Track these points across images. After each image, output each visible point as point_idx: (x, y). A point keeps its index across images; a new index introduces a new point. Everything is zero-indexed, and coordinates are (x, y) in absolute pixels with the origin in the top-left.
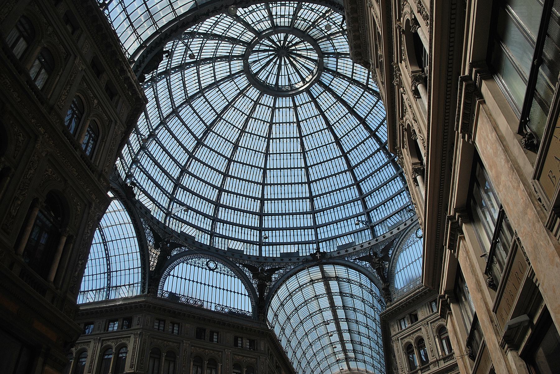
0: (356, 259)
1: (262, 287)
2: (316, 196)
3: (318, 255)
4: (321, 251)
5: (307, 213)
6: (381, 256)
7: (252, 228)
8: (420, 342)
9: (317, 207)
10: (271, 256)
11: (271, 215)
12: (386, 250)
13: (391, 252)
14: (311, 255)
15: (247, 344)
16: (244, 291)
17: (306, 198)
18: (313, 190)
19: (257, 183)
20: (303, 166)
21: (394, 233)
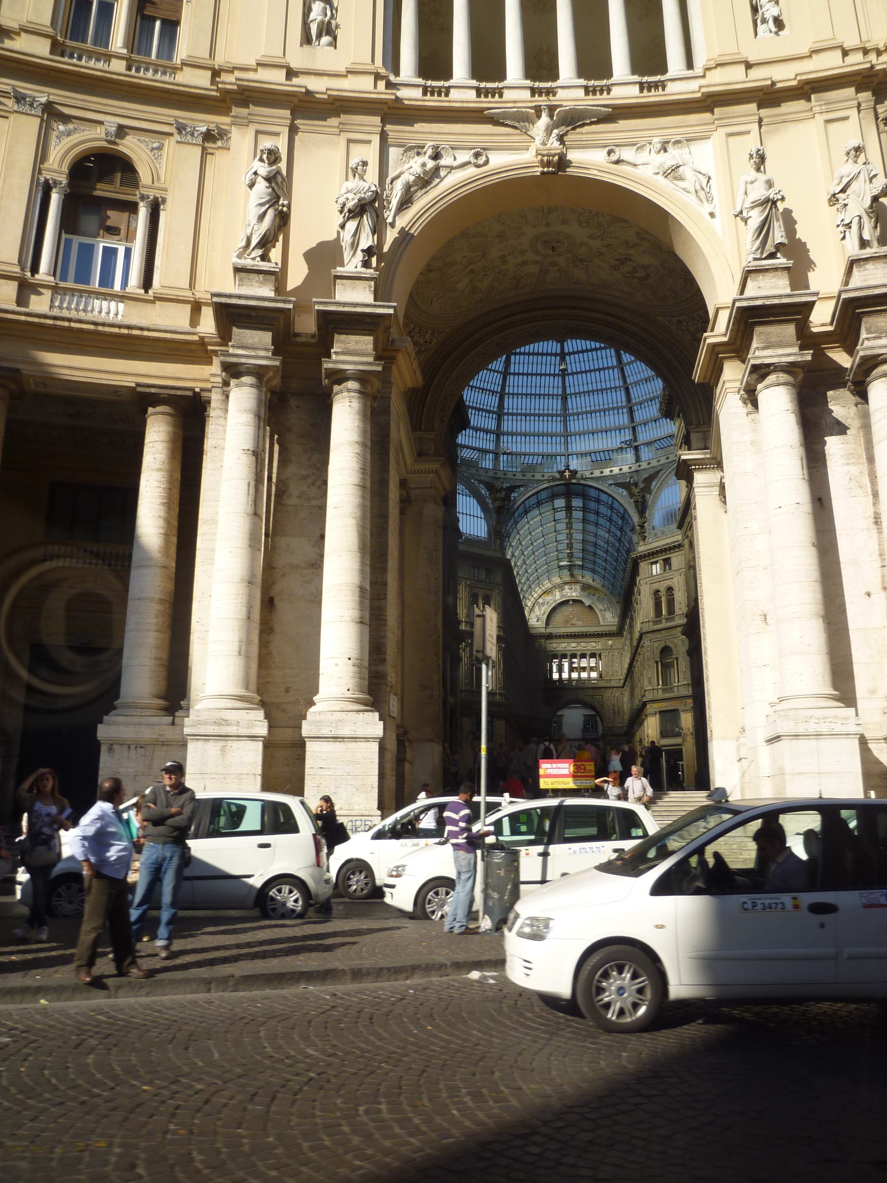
0: (611, 484)
1: (499, 510)
2: (571, 394)
3: (567, 474)
4: (571, 468)
5: (557, 415)
6: (641, 485)
7: (487, 431)
8: (670, 589)
9: (570, 407)
10: (510, 469)
11: (513, 414)
12: (649, 480)
13: (654, 483)
14: (559, 472)
15: (483, 575)
16: (480, 513)
17: (557, 395)
18: (567, 384)
19: (498, 372)
20: (559, 351)
21: (661, 462)
